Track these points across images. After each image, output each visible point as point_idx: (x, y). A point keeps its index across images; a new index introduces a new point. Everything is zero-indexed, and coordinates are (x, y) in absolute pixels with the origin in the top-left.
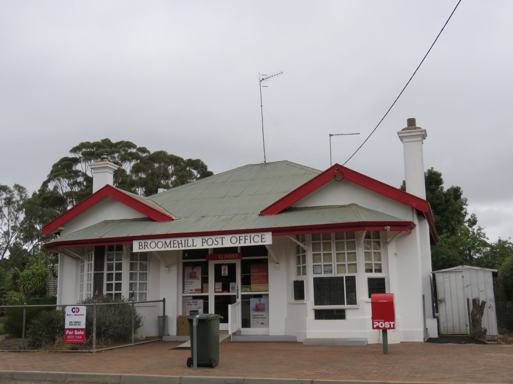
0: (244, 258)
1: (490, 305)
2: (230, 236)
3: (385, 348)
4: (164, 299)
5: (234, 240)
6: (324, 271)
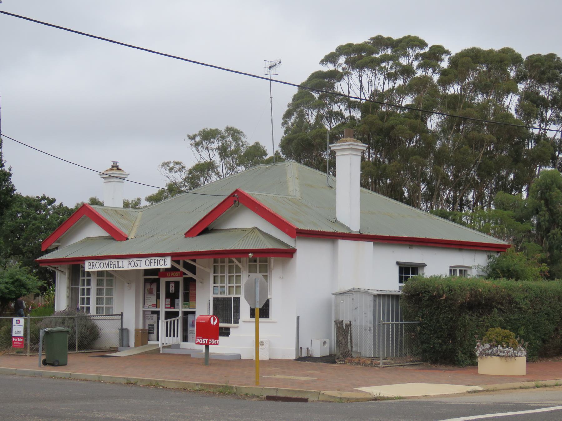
4: (122, 313)
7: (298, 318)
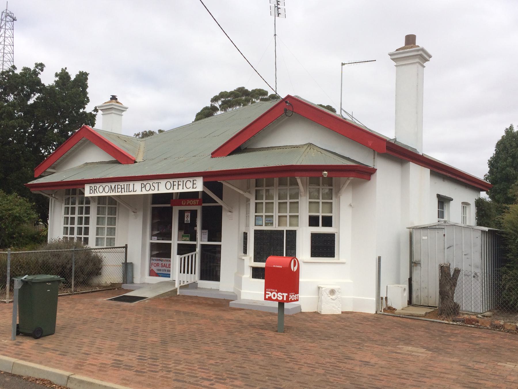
0: (204, 205)
1: (476, 274)
2: (166, 181)
3: (282, 323)
4: (126, 245)
5: (189, 184)
6: (266, 223)
7: (379, 258)
